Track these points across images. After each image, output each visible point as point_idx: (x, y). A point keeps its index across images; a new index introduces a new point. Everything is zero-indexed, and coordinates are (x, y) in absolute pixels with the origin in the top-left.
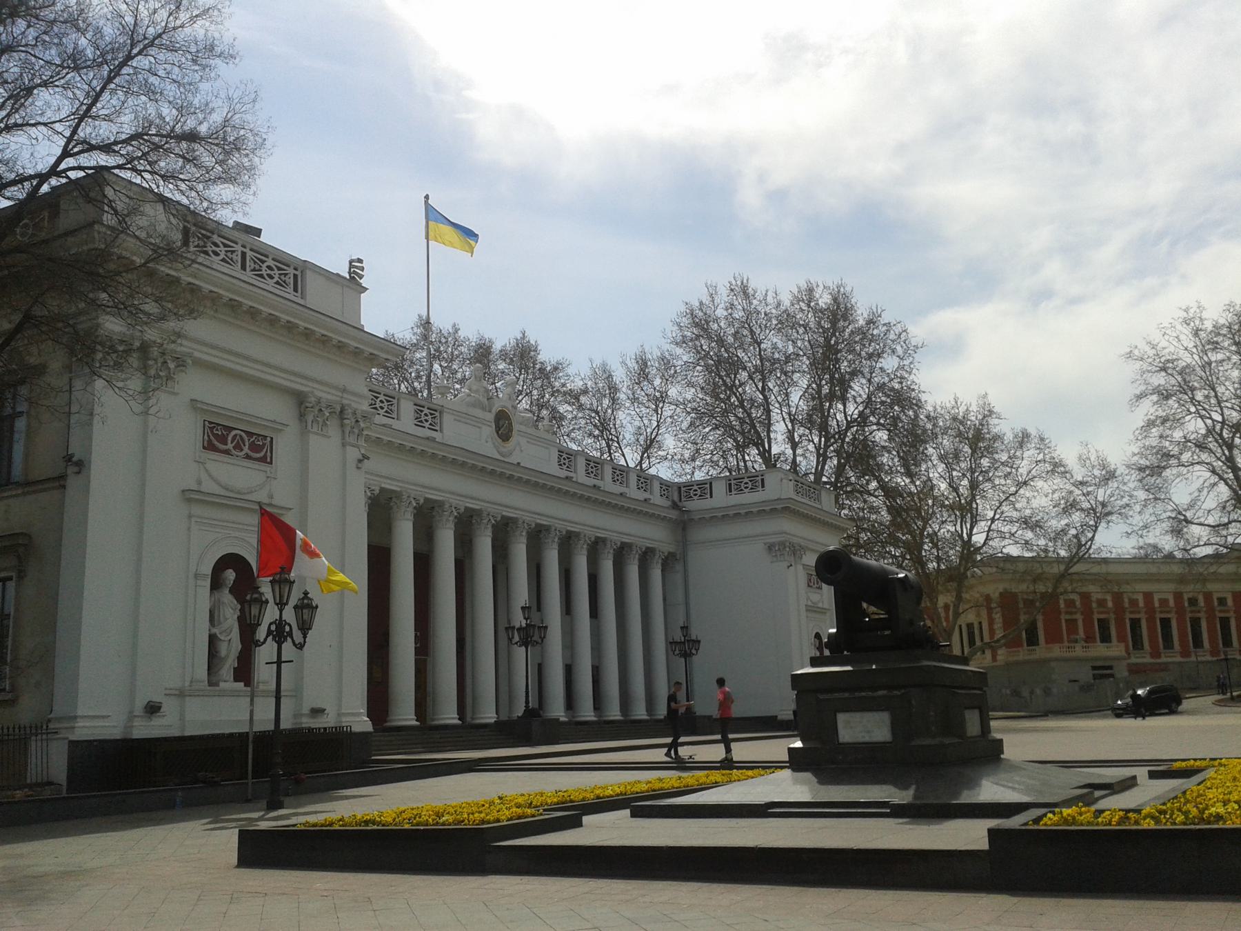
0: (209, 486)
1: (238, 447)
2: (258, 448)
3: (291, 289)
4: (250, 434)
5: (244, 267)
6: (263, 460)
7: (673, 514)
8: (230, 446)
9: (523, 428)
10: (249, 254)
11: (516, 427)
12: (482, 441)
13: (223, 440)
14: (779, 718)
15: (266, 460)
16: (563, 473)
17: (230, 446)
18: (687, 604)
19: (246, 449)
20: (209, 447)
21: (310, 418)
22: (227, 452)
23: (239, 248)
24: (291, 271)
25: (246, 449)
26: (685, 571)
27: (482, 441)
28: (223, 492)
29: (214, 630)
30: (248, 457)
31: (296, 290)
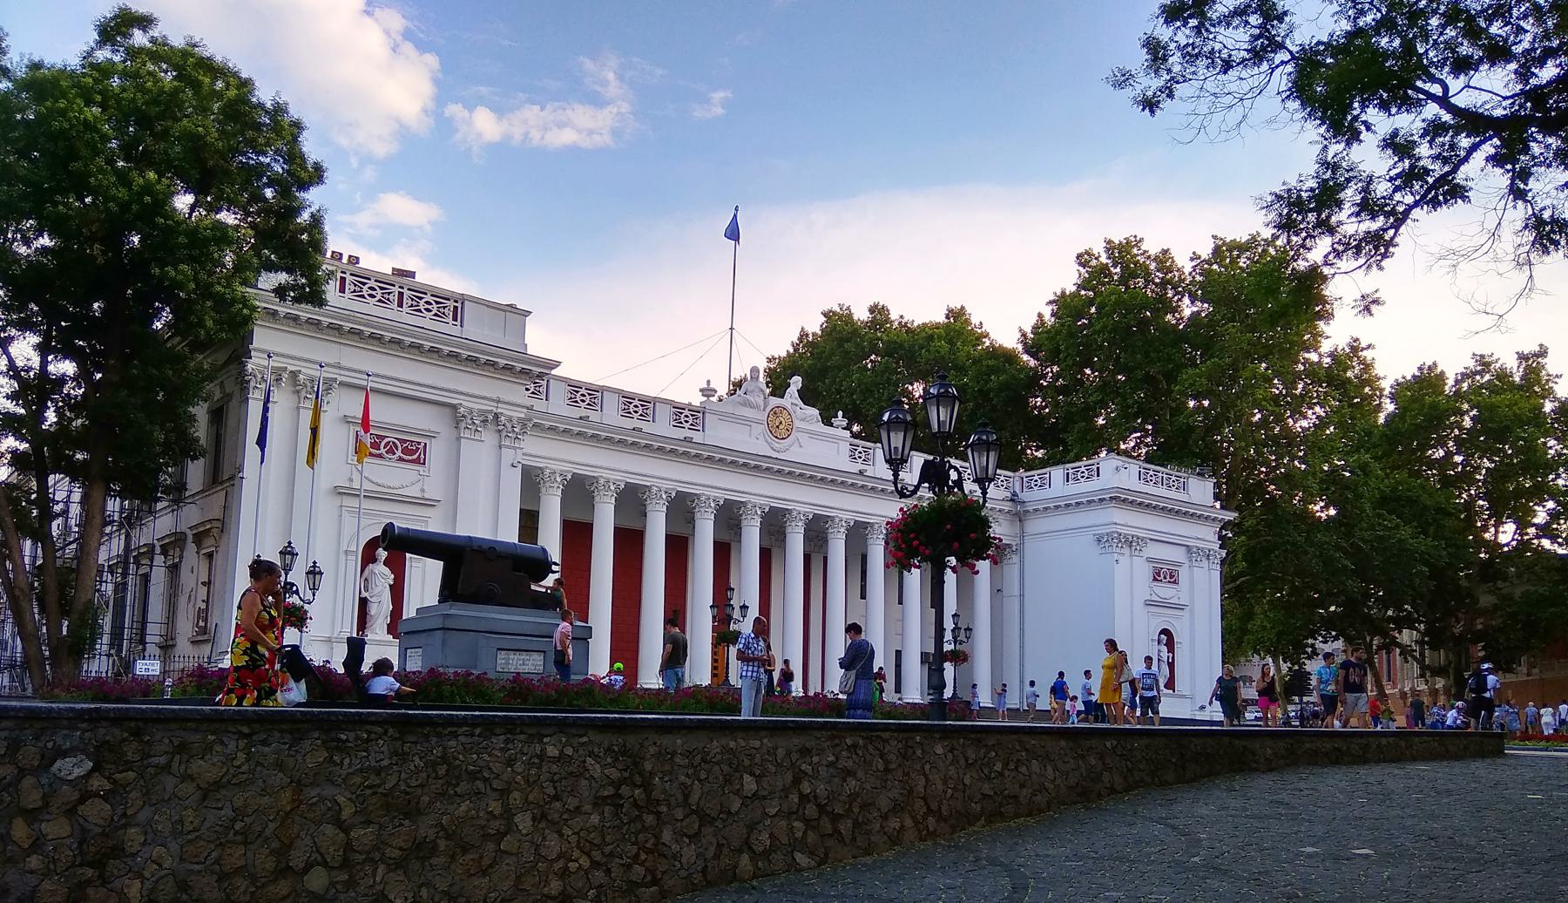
2: (412, 452)
3: (450, 320)
4: (403, 441)
5: (400, 305)
6: (417, 461)
7: (1007, 506)
8: (383, 451)
11: (797, 424)
15: (419, 462)
16: (855, 468)
18: (1022, 596)
19: (399, 453)
21: (463, 425)
22: (380, 456)
24: (451, 304)
25: (399, 453)
26: (1022, 562)
30: (401, 459)
31: (455, 319)
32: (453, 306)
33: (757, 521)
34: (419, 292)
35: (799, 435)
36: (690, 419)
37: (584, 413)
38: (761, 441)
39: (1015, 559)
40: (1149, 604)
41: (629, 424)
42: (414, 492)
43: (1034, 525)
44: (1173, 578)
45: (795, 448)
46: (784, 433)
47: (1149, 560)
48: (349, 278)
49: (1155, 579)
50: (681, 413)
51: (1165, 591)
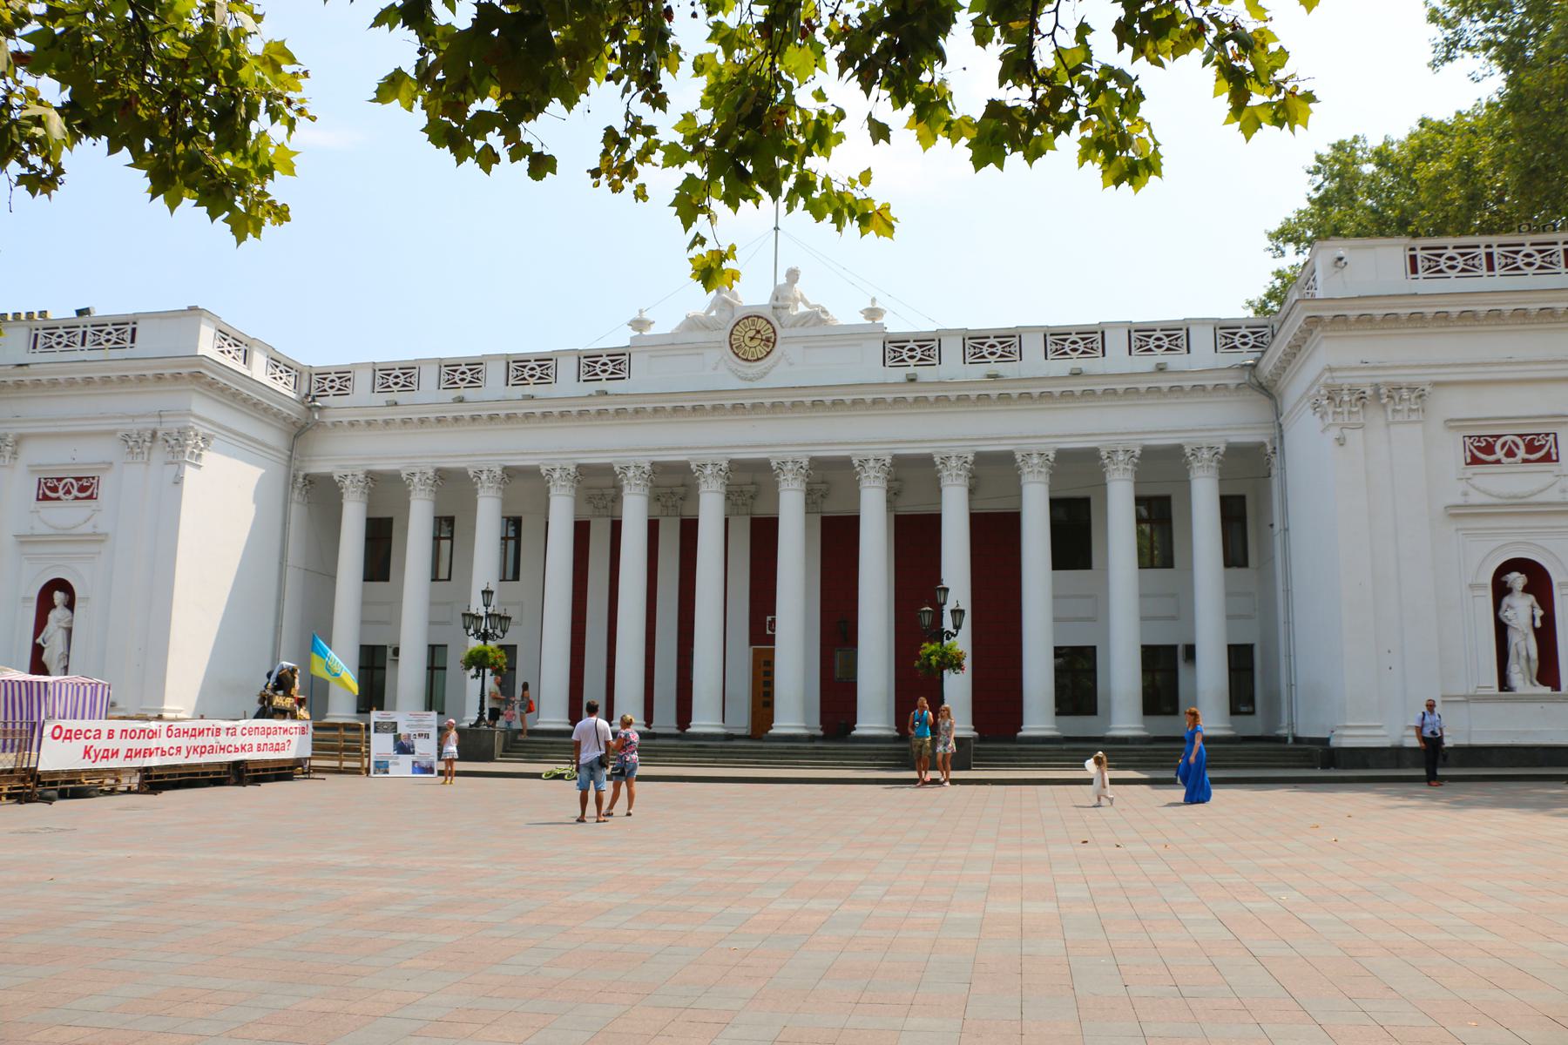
0: (41, 529)
1: (68, 492)
2: (86, 488)
6: (90, 497)
8: (61, 493)
9: (794, 332)
10: (90, 330)
11: (781, 333)
12: (718, 372)
13: (55, 489)
14: (1334, 743)
17: (61, 493)
19: (75, 492)
20: (46, 498)
22: (58, 499)
23: (80, 331)
24: (129, 328)
25: (75, 492)
27: (718, 372)
28: (52, 531)
29: (39, 640)
30: (77, 498)
32: (124, 330)
36: (610, 368)
40: (1458, 513)
42: (87, 528)
44: (1539, 449)
47: (1452, 424)
49: (1475, 461)
51: (1513, 480)
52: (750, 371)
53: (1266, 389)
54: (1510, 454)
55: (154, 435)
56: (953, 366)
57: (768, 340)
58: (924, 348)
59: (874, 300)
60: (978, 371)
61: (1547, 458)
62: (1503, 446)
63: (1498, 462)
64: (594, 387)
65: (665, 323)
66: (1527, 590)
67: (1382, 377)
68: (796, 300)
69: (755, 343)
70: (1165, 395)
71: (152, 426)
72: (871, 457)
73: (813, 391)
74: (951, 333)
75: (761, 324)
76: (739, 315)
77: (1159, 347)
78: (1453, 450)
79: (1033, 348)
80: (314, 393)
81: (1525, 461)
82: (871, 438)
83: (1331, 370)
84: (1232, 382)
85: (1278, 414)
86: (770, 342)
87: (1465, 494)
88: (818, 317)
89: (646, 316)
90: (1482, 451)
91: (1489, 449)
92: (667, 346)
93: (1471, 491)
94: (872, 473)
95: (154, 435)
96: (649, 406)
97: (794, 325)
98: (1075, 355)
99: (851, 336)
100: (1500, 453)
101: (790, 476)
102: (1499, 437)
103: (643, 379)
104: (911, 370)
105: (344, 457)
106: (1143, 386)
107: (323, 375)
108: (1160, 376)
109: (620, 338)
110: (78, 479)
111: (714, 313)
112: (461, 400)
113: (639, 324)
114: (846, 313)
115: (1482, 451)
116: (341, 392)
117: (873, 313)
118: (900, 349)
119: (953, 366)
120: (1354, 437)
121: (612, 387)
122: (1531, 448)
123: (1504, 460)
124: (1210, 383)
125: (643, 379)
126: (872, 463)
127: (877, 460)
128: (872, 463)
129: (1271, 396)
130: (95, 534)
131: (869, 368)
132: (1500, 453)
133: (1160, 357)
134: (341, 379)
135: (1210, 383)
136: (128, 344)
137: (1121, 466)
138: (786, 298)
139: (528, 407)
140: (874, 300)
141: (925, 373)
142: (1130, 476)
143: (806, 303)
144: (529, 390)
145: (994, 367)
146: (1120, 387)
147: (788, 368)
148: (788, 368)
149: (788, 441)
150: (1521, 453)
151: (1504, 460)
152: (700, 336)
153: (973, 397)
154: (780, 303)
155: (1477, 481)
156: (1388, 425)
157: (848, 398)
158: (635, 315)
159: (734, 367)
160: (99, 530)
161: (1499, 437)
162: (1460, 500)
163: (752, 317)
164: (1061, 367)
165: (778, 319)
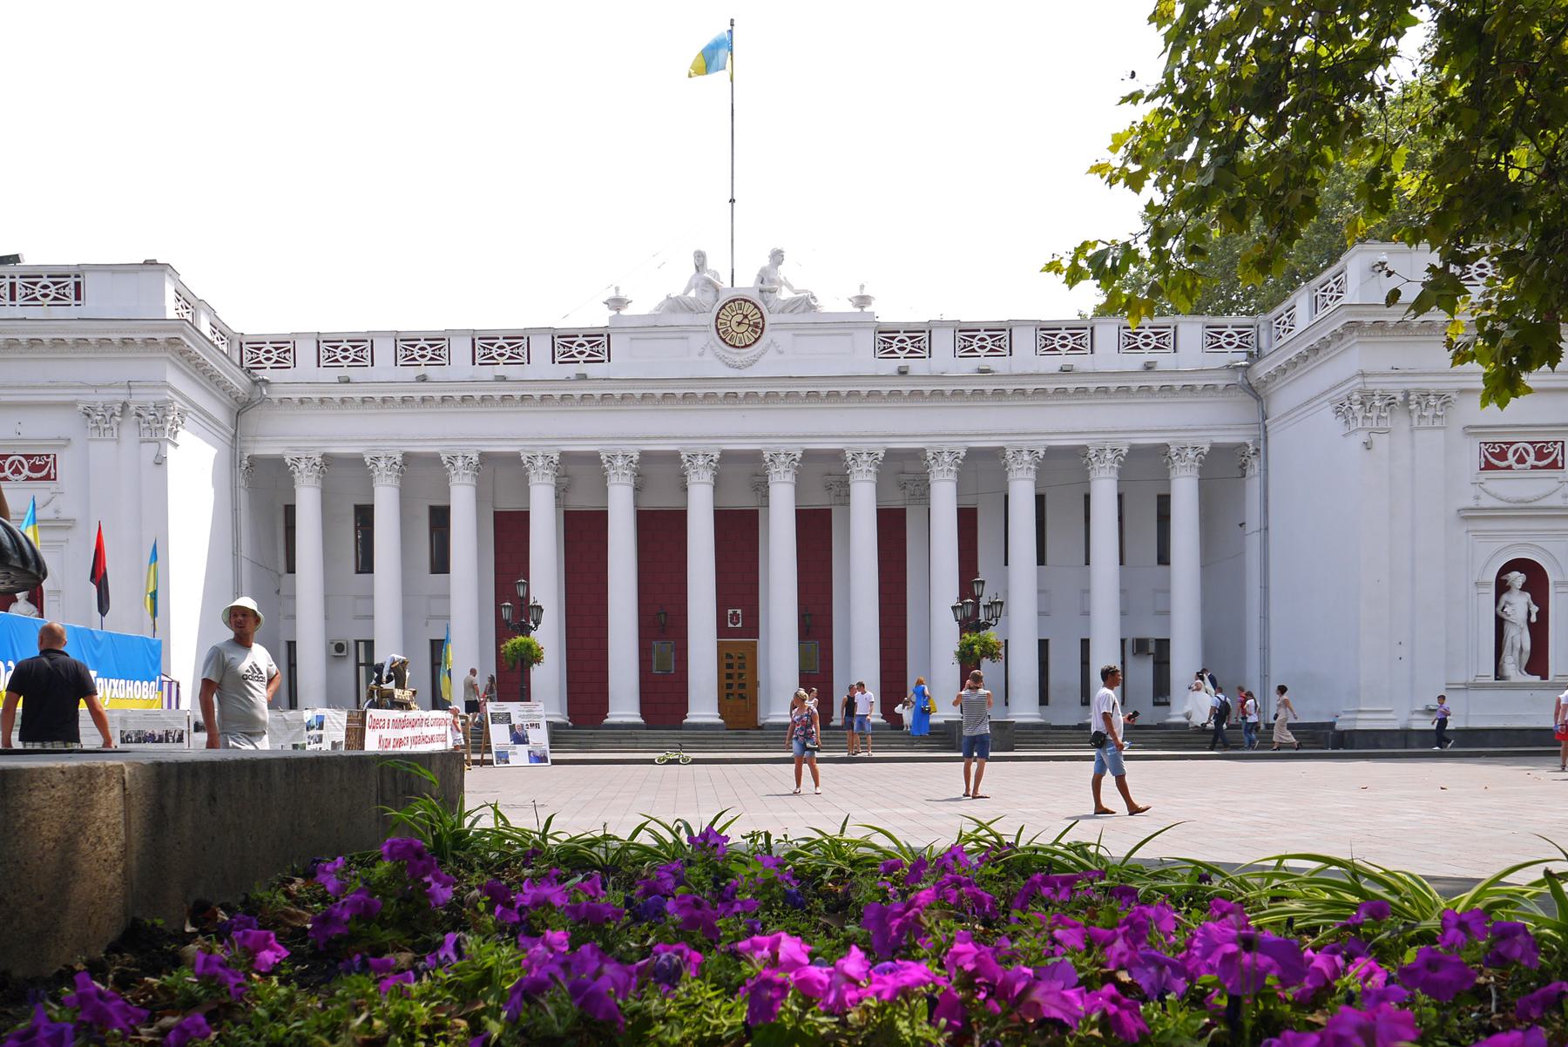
11: (769, 319)
12: (703, 358)
16: (890, 366)
27: (703, 358)
33: (707, 477)
34: (32, 277)
35: (774, 335)
37: (422, 370)
38: (709, 356)
39: (1255, 467)
41: (488, 372)
43: (1284, 399)
45: (771, 355)
46: (749, 337)
47: (1470, 430)
48: (19, 282)
49: (1489, 466)
50: (567, 344)
52: (738, 359)
53: (1255, 392)
54: (1521, 460)
55: (125, 406)
56: (943, 358)
57: (756, 325)
58: (916, 339)
59: (862, 287)
60: (969, 366)
61: (1553, 465)
62: (1515, 452)
63: (1509, 467)
64: (571, 370)
65: (643, 304)
66: (1524, 588)
67: (1412, 384)
68: (781, 284)
69: (743, 328)
70: (1154, 395)
71: (123, 398)
72: (865, 451)
73: (727, 383)
74: (942, 324)
75: (748, 309)
76: (724, 298)
77: (1147, 345)
78: (1471, 455)
79: (1024, 343)
80: (246, 364)
81: (1534, 467)
82: (865, 431)
83: (1363, 375)
84: (1221, 383)
85: (1265, 418)
86: (758, 328)
87: (1477, 498)
88: (808, 303)
89: (622, 294)
90: (1495, 458)
91: (1502, 456)
92: (647, 329)
93: (1483, 495)
94: (865, 467)
95: (125, 406)
96: (537, 394)
97: (782, 311)
98: (1064, 351)
99: (841, 326)
100: (1511, 459)
101: (782, 469)
102: (1512, 444)
103: (624, 362)
104: (902, 362)
105: (288, 437)
106: (1135, 385)
107: (257, 344)
108: (1149, 376)
109: (599, 318)
110: (28, 457)
111: (692, 294)
112: (423, 379)
113: (617, 303)
114: (834, 301)
115: (1495, 458)
116: (279, 365)
117: (863, 301)
118: (889, 339)
119: (943, 358)
120: (1381, 442)
121: (592, 370)
122: (1540, 455)
123: (1515, 466)
124: (1199, 383)
125: (624, 362)
126: (865, 457)
127: (870, 454)
128: (865, 457)
129: (1258, 398)
130: (57, 519)
131: (862, 358)
132: (1511, 459)
133: (1147, 355)
134: (283, 350)
135: (1199, 383)
136: (72, 300)
137: (1108, 464)
138: (772, 281)
139: (498, 391)
140: (862, 287)
141: (917, 366)
142: (1195, 472)
143: (790, 287)
144: (501, 370)
145: (984, 362)
146: (1113, 386)
147: (776, 357)
148: (776, 357)
149: (780, 432)
150: (1531, 460)
151: (1515, 466)
152: (683, 319)
153: (968, 392)
154: (766, 286)
155: (1489, 486)
156: (1412, 431)
157: (844, 390)
158: (612, 294)
159: (722, 353)
160: (63, 515)
161: (1512, 444)
162: (1472, 504)
163: (739, 301)
164: (1052, 363)
165: (766, 303)
